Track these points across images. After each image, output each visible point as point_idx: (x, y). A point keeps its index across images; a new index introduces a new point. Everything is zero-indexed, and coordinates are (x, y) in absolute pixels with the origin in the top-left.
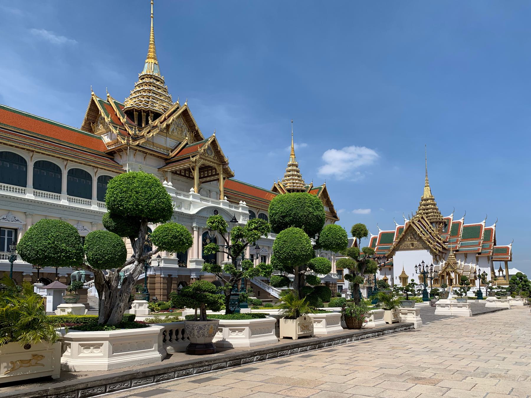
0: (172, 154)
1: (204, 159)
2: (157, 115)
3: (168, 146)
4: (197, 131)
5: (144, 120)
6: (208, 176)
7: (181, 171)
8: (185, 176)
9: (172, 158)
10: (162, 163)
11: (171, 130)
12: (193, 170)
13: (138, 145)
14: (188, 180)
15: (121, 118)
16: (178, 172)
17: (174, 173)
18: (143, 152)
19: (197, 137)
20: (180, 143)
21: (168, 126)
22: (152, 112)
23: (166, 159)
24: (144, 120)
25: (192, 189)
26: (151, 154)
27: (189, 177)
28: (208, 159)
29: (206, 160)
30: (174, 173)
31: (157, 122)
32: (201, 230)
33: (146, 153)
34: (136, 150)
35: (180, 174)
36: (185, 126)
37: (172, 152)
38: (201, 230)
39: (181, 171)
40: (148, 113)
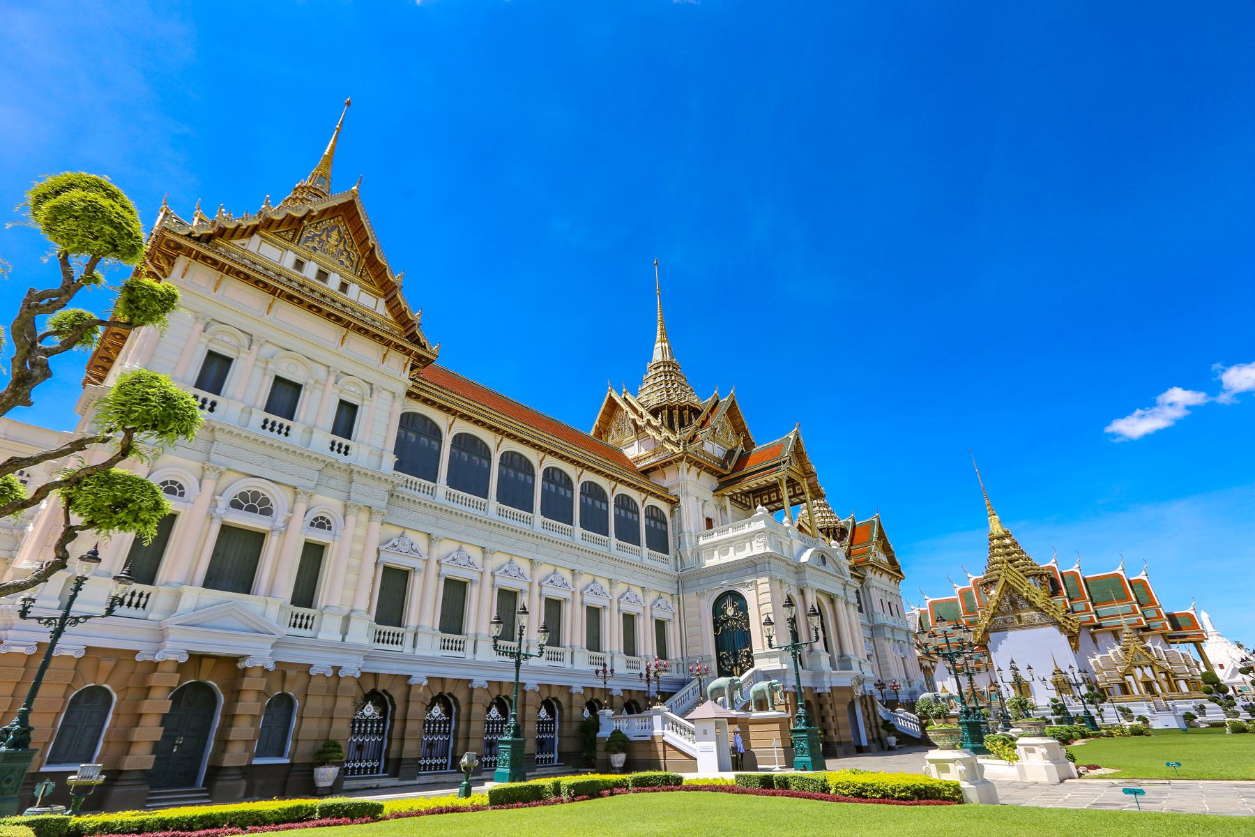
8: (741, 503)
40: (682, 409)
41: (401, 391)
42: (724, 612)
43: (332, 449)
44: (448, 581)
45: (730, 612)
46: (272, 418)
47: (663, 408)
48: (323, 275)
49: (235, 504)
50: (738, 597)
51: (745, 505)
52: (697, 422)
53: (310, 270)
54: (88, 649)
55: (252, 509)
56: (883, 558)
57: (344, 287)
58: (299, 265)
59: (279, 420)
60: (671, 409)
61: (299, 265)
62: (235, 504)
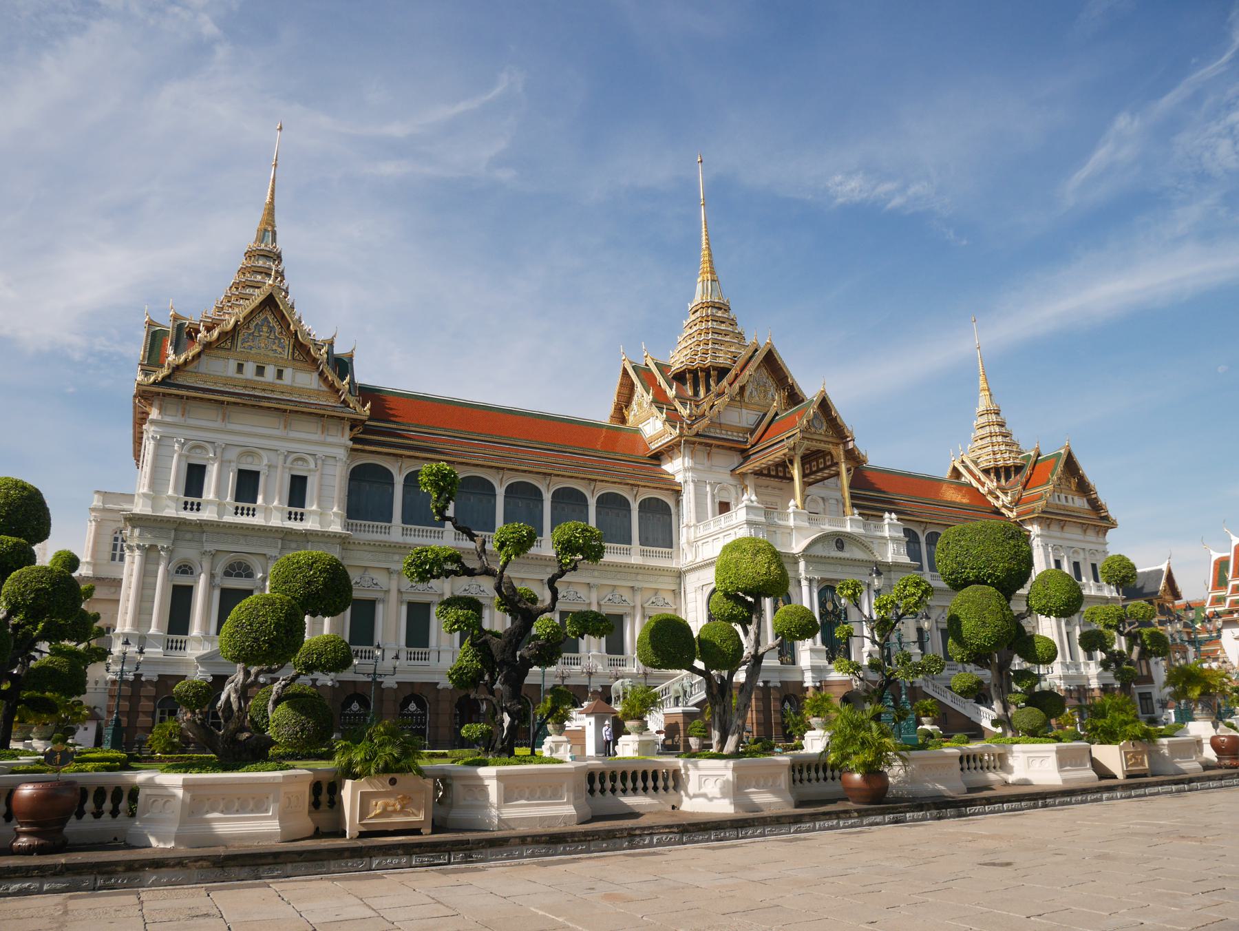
1: (808, 439)
2: (722, 372)
3: (744, 424)
4: (792, 387)
6: (819, 470)
7: (769, 470)
8: (777, 476)
10: (736, 459)
11: (747, 393)
12: (791, 462)
14: (784, 484)
15: (668, 390)
18: (707, 445)
19: (794, 397)
20: (765, 415)
21: (742, 388)
22: (715, 368)
25: (792, 503)
26: (718, 446)
27: (784, 478)
29: (812, 440)
30: (758, 473)
31: (725, 382)
32: (815, 584)
33: (710, 446)
34: (694, 443)
35: (769, 475)
36: (770, 382)
37: (751, 435)
38: (815, 584)
39: (769, 470)
41: (341, 454)
43: (290, 518)
44: (411, 606)
46: (240, 505)
47: (684, 371)
48: (260, 370)
49: (227, 574)
53: (250, 370)
54: (159, 676)
55: (239, 575)
56: (1080, 503)
57: (280, 374)
58: (240, 367)
59: (246, 505)
60: (694, 372)
61: (240, 367)
62: (227, 574)
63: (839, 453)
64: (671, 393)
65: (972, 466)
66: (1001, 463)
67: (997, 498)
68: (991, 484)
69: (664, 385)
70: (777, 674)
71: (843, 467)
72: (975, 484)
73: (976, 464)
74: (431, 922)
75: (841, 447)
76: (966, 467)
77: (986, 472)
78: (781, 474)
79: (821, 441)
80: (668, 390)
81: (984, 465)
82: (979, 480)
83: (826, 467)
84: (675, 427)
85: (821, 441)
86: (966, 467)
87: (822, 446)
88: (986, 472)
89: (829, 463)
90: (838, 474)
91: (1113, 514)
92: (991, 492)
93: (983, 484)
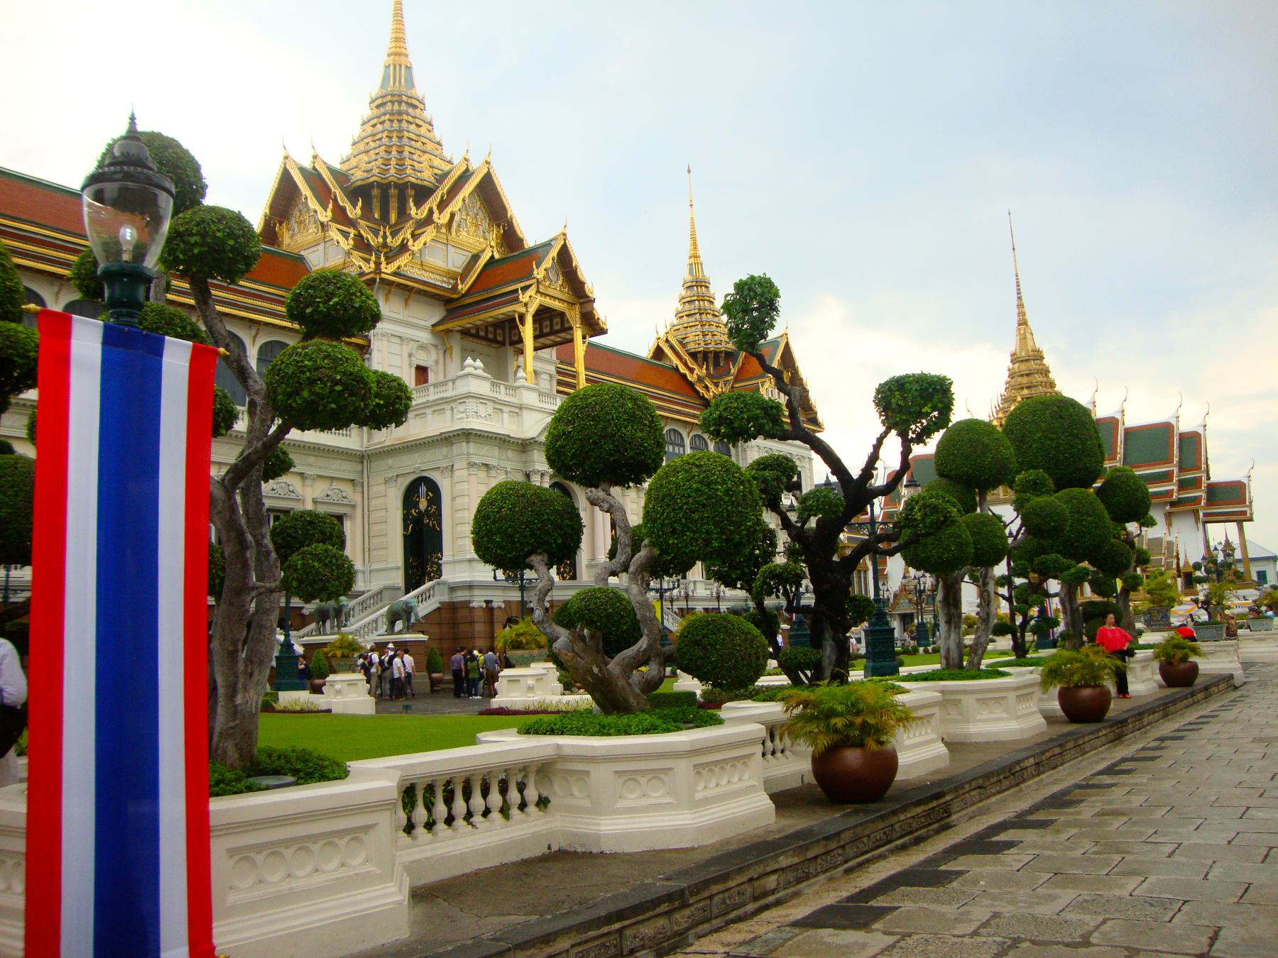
0: (463, 287)
3: (451, 267)
5: (394, 204)
9: (463, 296)
11: (454, 225)
12: (523, 323)
13: (395, 274)
15: (348, 207)
16: (473, 331)
17: (465, 333)
18: (405, 287)
22: (414, 186)
23: (448, 301)
24: (394, 204)
26: (419, 292)
28: (551, 292)
30: (465, 333)
34: (390, 283)
35: (477, 336)
39: (478, 330)
40: (402, 188)
42: (416, 505)
45: (423, 505)
47: (371, 185)
50: (433, 487)
51: (495, 341)
52: (416, 213)
60: (384, 188)
63: (574, 317)
64: (354, 212)
65: (678, 347)
66: (712, 347)
67: (706, 387)
68: (700, 371)
69: (343, 201)
70: (499, 593)
71: (578, 334)
72: (683, 370)
73: (683, 345)
74: (640, 918)
75: (577, 307)
76: (672, 347)
77: (693, 355)
78: (491, 336)
79: (555, 298)
80: (348, 207)
81: (692, 347)
82: (686, 364)
83: (553, 333)
84: (368, 261)
85: (555, 298)
86: (672, 347)
87: (557, 305)
88: (693, 355)
89: (557, 327)
90: (572, 340)
91: (820, 417)
92: (700, 379)
93: (692, 370)
